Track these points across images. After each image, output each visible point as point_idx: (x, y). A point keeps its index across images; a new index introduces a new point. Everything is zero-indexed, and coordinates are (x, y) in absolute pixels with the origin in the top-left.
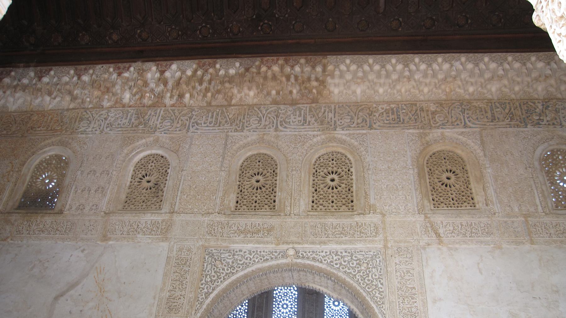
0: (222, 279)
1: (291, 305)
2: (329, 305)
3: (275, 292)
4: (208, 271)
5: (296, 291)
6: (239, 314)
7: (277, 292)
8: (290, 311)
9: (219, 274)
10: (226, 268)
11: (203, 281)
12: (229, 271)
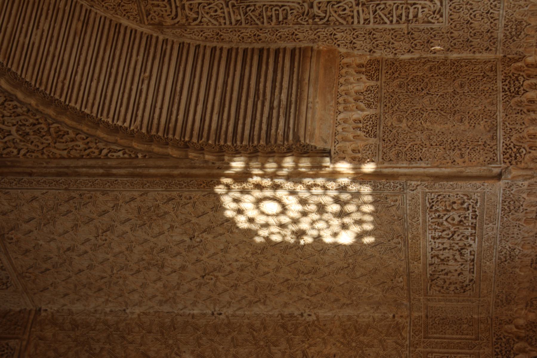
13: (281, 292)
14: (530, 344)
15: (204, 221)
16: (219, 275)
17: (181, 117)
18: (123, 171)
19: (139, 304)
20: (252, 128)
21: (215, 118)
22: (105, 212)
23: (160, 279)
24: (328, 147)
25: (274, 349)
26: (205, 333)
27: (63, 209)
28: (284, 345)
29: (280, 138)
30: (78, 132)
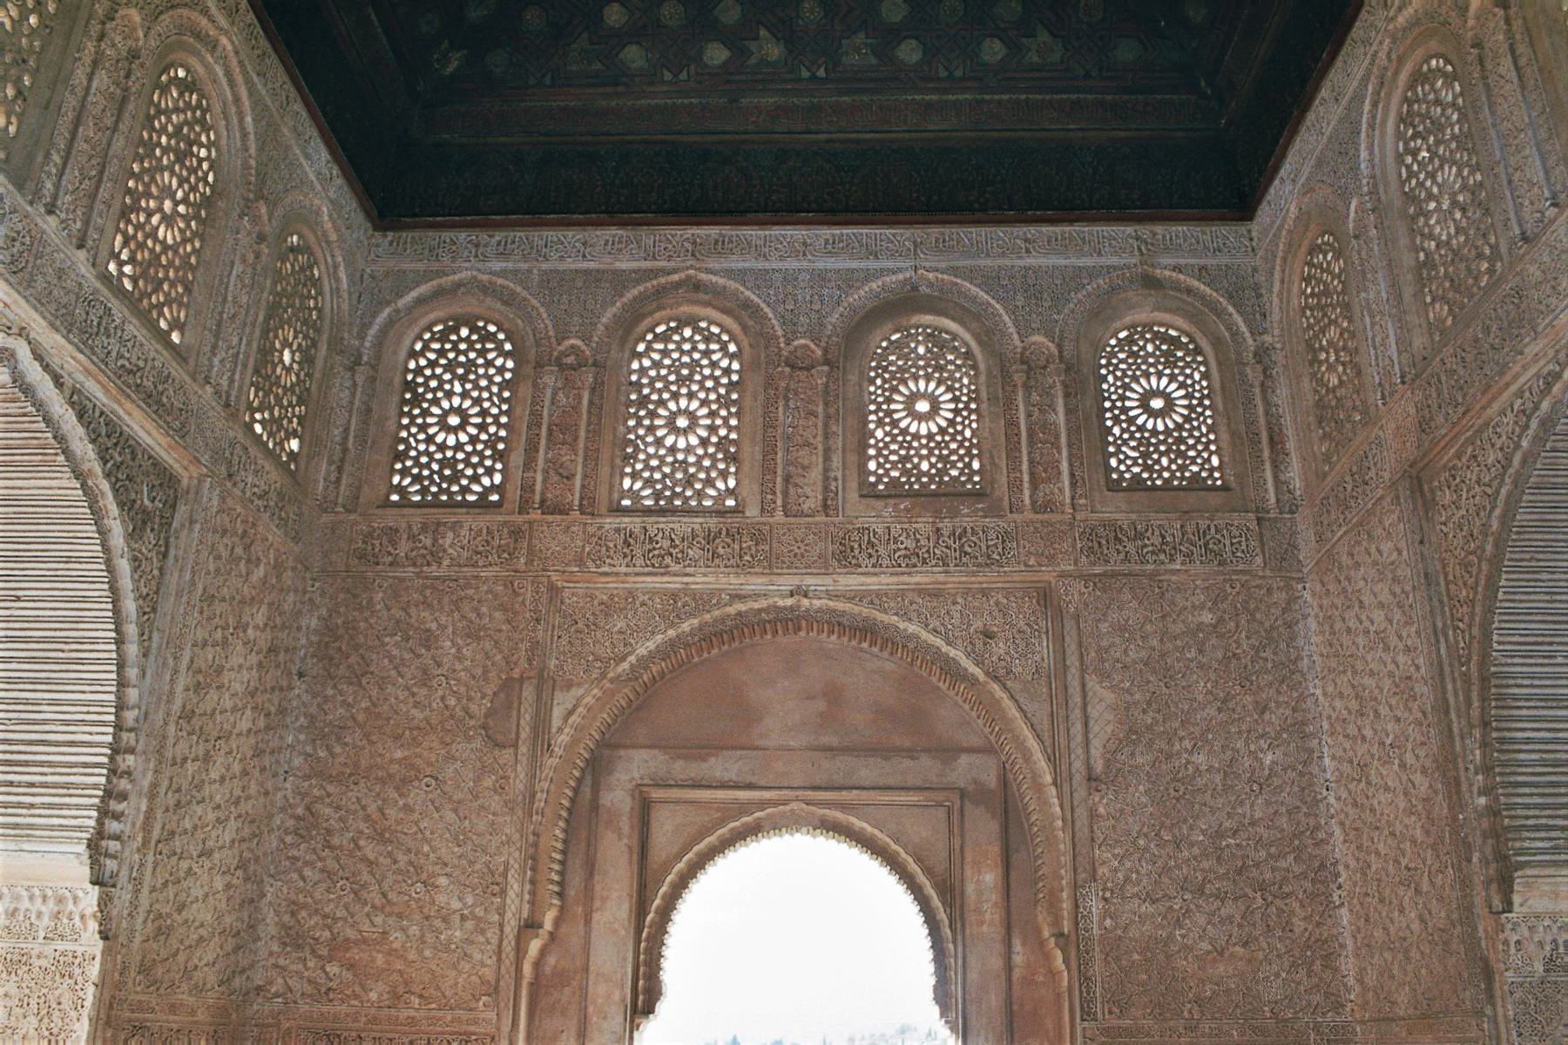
1: (712, 414)
2: (889, 413)
3: (635, 365)
5: (732, 357)
7: (646, 363)
13: (1358, 860)
15: (1409, 759)
16: (1363, 785)
17: (1524, 712)
18: (1443, 651)
19: (1325, 694)
20: (1527, 806)
21: (1534, 756)
22: (1400, 637)
23: (1350, 713)
24: (1516, 907)
25: (1291, 858)
26: (1301, 774)
27: (1398, 590)
28: (1297, 869)
29: (1518, 844)
30: (1474, 588)
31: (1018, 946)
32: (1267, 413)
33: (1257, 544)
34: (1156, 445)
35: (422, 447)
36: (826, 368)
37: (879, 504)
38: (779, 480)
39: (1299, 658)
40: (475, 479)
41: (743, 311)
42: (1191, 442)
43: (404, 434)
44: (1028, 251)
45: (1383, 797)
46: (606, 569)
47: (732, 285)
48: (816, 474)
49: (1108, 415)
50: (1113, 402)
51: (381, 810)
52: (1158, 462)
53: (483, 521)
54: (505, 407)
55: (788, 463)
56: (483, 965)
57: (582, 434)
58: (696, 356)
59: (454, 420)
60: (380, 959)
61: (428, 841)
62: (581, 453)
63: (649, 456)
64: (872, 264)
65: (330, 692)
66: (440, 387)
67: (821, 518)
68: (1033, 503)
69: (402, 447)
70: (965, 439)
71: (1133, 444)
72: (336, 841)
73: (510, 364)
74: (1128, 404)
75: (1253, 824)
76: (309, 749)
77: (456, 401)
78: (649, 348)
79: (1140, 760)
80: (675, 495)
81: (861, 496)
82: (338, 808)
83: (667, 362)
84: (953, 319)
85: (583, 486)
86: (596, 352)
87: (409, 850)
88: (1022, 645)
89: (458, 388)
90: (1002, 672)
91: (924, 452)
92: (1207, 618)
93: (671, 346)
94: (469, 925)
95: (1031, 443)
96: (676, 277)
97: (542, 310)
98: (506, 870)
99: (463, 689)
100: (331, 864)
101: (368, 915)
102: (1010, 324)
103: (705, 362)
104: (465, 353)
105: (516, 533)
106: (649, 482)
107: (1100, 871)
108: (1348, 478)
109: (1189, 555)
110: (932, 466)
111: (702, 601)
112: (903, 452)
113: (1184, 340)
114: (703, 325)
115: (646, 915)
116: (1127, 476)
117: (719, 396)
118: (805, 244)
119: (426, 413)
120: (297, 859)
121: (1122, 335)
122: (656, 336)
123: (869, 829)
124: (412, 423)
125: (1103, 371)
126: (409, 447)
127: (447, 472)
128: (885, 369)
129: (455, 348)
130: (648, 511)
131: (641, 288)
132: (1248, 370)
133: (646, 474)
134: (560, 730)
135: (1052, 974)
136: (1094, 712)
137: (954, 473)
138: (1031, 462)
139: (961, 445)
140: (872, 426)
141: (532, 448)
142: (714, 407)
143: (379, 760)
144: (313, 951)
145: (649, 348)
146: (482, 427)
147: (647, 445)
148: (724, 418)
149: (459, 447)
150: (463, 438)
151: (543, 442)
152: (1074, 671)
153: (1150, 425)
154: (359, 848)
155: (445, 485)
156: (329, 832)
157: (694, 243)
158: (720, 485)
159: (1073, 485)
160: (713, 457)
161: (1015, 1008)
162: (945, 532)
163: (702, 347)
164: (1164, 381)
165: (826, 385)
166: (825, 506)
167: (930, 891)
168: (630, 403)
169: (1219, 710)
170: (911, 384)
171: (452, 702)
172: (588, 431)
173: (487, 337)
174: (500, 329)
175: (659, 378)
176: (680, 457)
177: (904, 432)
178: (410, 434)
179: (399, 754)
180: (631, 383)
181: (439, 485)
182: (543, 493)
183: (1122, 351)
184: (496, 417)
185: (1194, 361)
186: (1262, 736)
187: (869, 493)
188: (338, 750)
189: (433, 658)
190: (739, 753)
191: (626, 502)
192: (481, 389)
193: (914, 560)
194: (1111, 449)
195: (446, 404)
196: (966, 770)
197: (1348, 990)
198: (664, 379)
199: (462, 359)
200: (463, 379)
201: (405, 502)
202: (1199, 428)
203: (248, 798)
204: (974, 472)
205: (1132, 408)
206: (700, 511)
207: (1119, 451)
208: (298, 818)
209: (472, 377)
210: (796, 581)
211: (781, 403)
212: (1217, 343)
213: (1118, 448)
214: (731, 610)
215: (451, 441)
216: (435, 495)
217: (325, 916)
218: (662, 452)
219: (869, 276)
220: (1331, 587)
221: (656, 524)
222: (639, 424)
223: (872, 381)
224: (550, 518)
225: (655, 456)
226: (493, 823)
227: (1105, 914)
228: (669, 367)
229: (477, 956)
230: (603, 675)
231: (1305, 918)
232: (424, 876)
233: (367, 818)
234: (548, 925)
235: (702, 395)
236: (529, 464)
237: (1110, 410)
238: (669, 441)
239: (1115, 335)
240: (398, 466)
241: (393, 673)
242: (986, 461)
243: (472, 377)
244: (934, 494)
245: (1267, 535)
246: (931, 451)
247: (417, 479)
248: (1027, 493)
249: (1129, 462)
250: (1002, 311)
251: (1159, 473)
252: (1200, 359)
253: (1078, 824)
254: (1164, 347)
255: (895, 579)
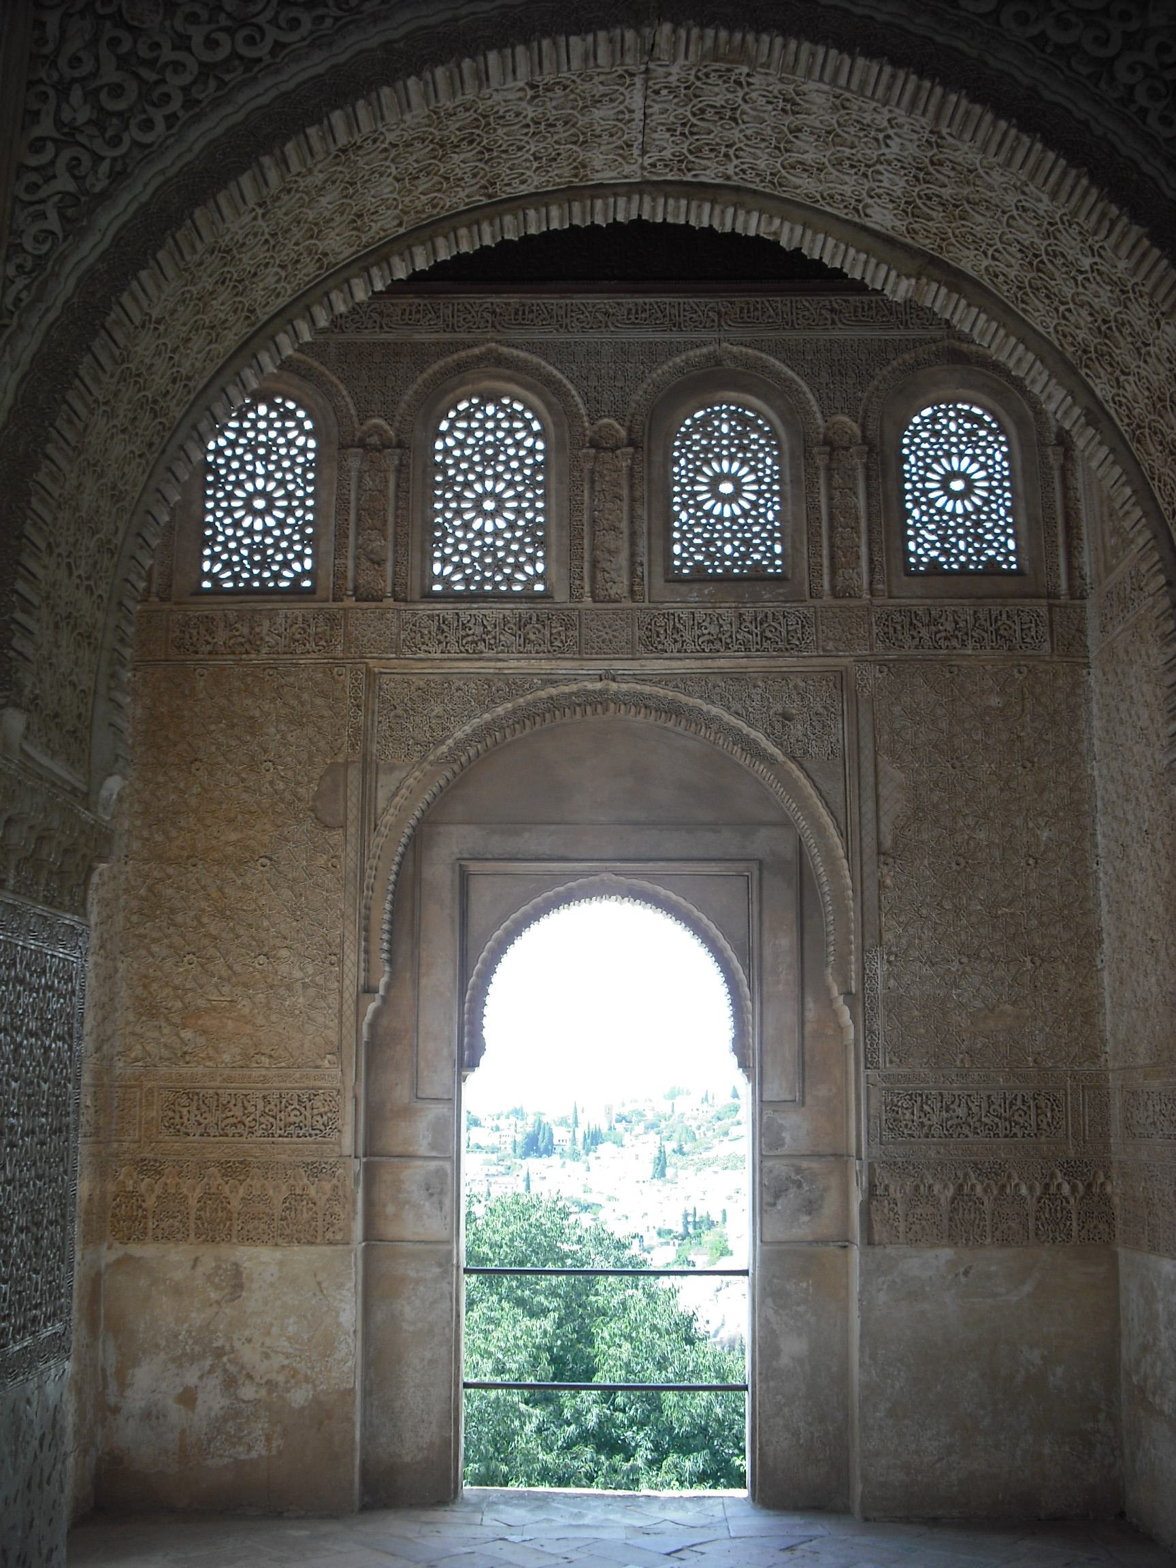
0: (176, 105)
1: (519, 497)
2: (694, 495)
3: (439, 445)
4: (75, 61)
5: (536, 435)
6: (276, 546)
7: (450, 442)
8: (512, 526)
9: (149, 76)
10: (197, 35)
11: (45, 127)
12: (223, 53)
14: (1083, 1198)
26: (1074, 850)
31: (810, 1004)
32: (1065, 496)
33: (1046, 630)
34: (954, 529)
35: (229, 532)
36: (631, 450)
37: (683, 588)
38: (586, 566)
39: (1080, 740)
40: (286, 564)
41: (545, 389)
42: (989, 525)
43: (210, 519)
44: (833, 323)
45: (1139, 876)
46: (422, 655)
47: (535, 359)
48: (623, 559)
49: (908, 497)
50: (914, 483)
51: (220, 889)
52: (955, 545)
53: (300, 609)
54: (310, 489)
55: (594, 548)
56: (327, 1027)
57: (391, 519)
58: (500, 435)
59: (259, 504)
60: (230, 1025)
61: (268, 918)
62: (390, 538)
63: (458, 541)
64: (675, 336)
65: (161, 779)
66: (242, 469)
67: (627, 604)
68: (833, 587)
69: (209, 532)
70: (768, 522)
71: (932, 527)
72: (179, 918)
73: (312, 444)
74: (928, 485)
75: (1027, 894)
76: (146, 834)
77: (260, 483)
78: (453, 427)
79: (925, 837)
80: (485, 580)
81: (667, 581)
82: (179, 888)
83: (471, 441)
84: (757, 396)
85: (395, 573)
86: (399, 432)
87: (250, 926)
88: (818, 726)
89: (260, 470)
90: (798, 753)
91: (727, 535)
92: (995, 701)
93: (475, 425)
94: (312, 992)
95: (832, 528)
96: (476, 351)
97: (342, 387)
98: (343, 942)
99: (290, 774)
100: (177, 940)
101: (216, 986)
102: (813, 402)
103: (509, 441)
104: (265, 432)
105: (332, 620)
106: (459, 567)
107: (888, 936)
108: (1128, 580)
109: (980, 641)
110: (736, 549)
111: (515, 685)
112: (706, 535)
113: (987, 418)
114: (506, 401)
115: (468, 979)
116: (925, 560)
117: (525, 477)
118: (606, 313)
119: (230, 496)
120: (145, 936)
121: (927, 412)
122: (458, 412)
123: (674, 897)
124: (217, 507)
125: (905, 451)
126: (216, 532)
127: (257, 558)
128: (689, 449)
129: (254, 427)
130: (459, 597)
131: (441, 363)
132: (1049, 450)
133: (456, 559)
134: (385, 810)
135: (840, 1029)
136: (884, 792)
137: (757, 556)
138: (832, 546)
139: (764, 529)
140: (676, 508)
141: (341, 534)
142: (520, 489)
143: (214, 842)
144: (167, 1020)
145: (453, 427)
146: (289, 511)
147: (455, 528)
148: (529, 500)
149: (267, 531)
150: (270, 522)
151: (352, 526)
152: (867, 753)
153: (949, 508)
154: (203, 926)
155: (256, 572)
156: (172, 911)
157: (494, 313)
158: (529, 569)
159: (872, 571)
160: (520, 540)
161: (807, 1057)
162: (747, 618)
163: (505, 425)
164: (966, 460)
165: (631, 469)
166: (632, 592)
167: (730, 953)
168: (438, 485)
169: (1002, 790)
170: (715, 465)
171: (281, 786)
172: (396, 516)
173: (287, 415)
174: (300, 406)
175: (463, 458)
176: (489, 540)
177: (708, 514)
178: (216, 519)
179: (233, 837)
180: (436, 464)
181: (250, 571)
182: (355, 580)
183: (925, 429)
184: (302, 500)
185: (996, 441)
186: (1040, 814)
187: (674, 578)
188: (174, 834)
189: (259, 745)
190: (553, 827)
191: (437, 588)
192: (285, 470)
193: (718, 646)
194: (910, 532)
195: (249, 487)
196: (763, 842)
197: (1104, 1042)
198: (468, 459)
199: (262, 438)
200: (266, 459)
201: (217, 589)
202: (997, 511)
203: (104, 884)
204: (776, 556)
205: (932, 490)
206: (510, 597)
207: (918, 535)
208: (142, 899)
209: (274, 457)
210: (604, 665)
211: (586, 486)
212: (1021, 423)
213: (917, 530)
214: (543, 694)
215: (258, 525)
216: (248, 582)
217: (176, 988)
218: (470, 536)
219: (674, 349)
220: (1110, 677)
221: (467, 611)
222: (446, 508)
223: (676, 462)
224: (365, 605)
225: (464, 540)
226: (327, 900)
227: (890, 975)
228: (473, 446)
229: (321, 1020)
230: (424, 758)
231: (1070, 980)
232: (265, 949)
233: (208, 897)
234: (381, 992)
235: (507, 477)
236: (340, 550)
237: (911, 492)
238: (477, 525)
239: (917, 413)
240: (207, 552)
241: (221, 759)
242: (789, 545)
243: (274, 457)
244: (739, 579)
245: (1057, 618)
246: (734, 533)
247: (228, 565)
248: (826, 578)
249: (927, 546)
250: (805, 388)
251: (956, 556)
252: (1002, 438)
253: (867, 894)
254: (967, 426)
255: (698, 663)
